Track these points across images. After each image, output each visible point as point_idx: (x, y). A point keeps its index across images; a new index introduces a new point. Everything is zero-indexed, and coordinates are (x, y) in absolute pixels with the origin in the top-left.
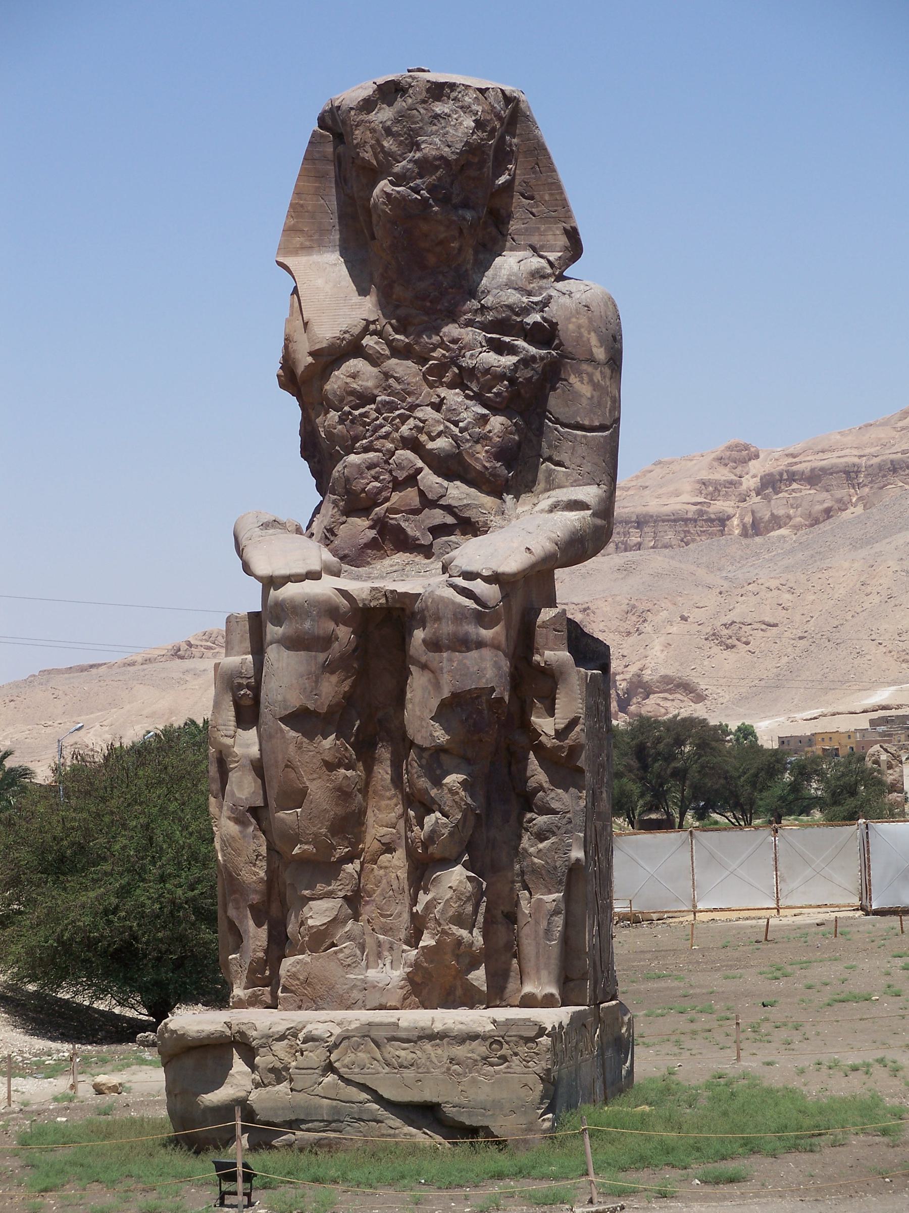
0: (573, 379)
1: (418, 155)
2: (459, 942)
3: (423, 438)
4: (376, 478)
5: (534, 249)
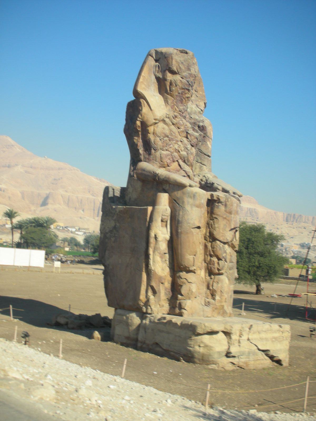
0: (208, 143)
1: (190, 72)
4: (169, 159)
5: (197, 105)
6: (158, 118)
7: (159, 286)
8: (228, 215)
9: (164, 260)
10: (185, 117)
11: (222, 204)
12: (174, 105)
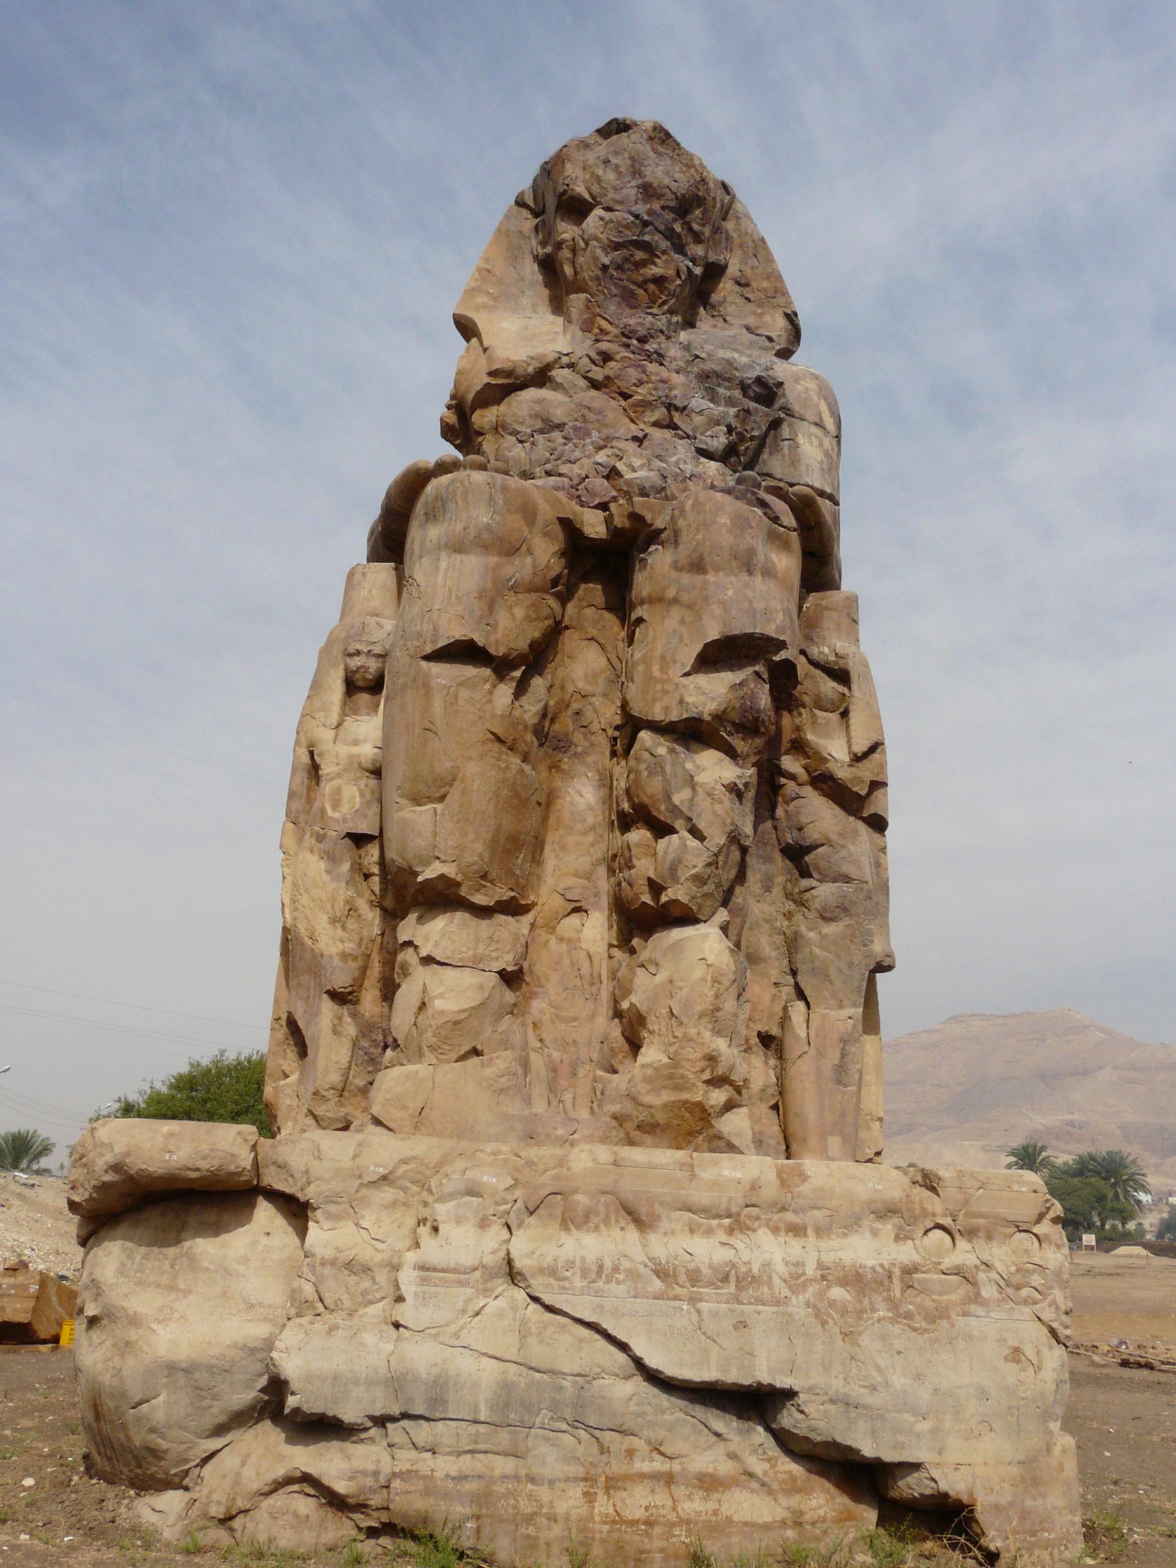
0: (801, 439)
2: (712, 1059)
3: (620, 466)
5: (748, 329)
6: (507, 366)
7: (317, 1013)
8: (687, 578)
9: (346, 867)
10: (661, 355)
11: (662, 544)
12: (595, 315)
